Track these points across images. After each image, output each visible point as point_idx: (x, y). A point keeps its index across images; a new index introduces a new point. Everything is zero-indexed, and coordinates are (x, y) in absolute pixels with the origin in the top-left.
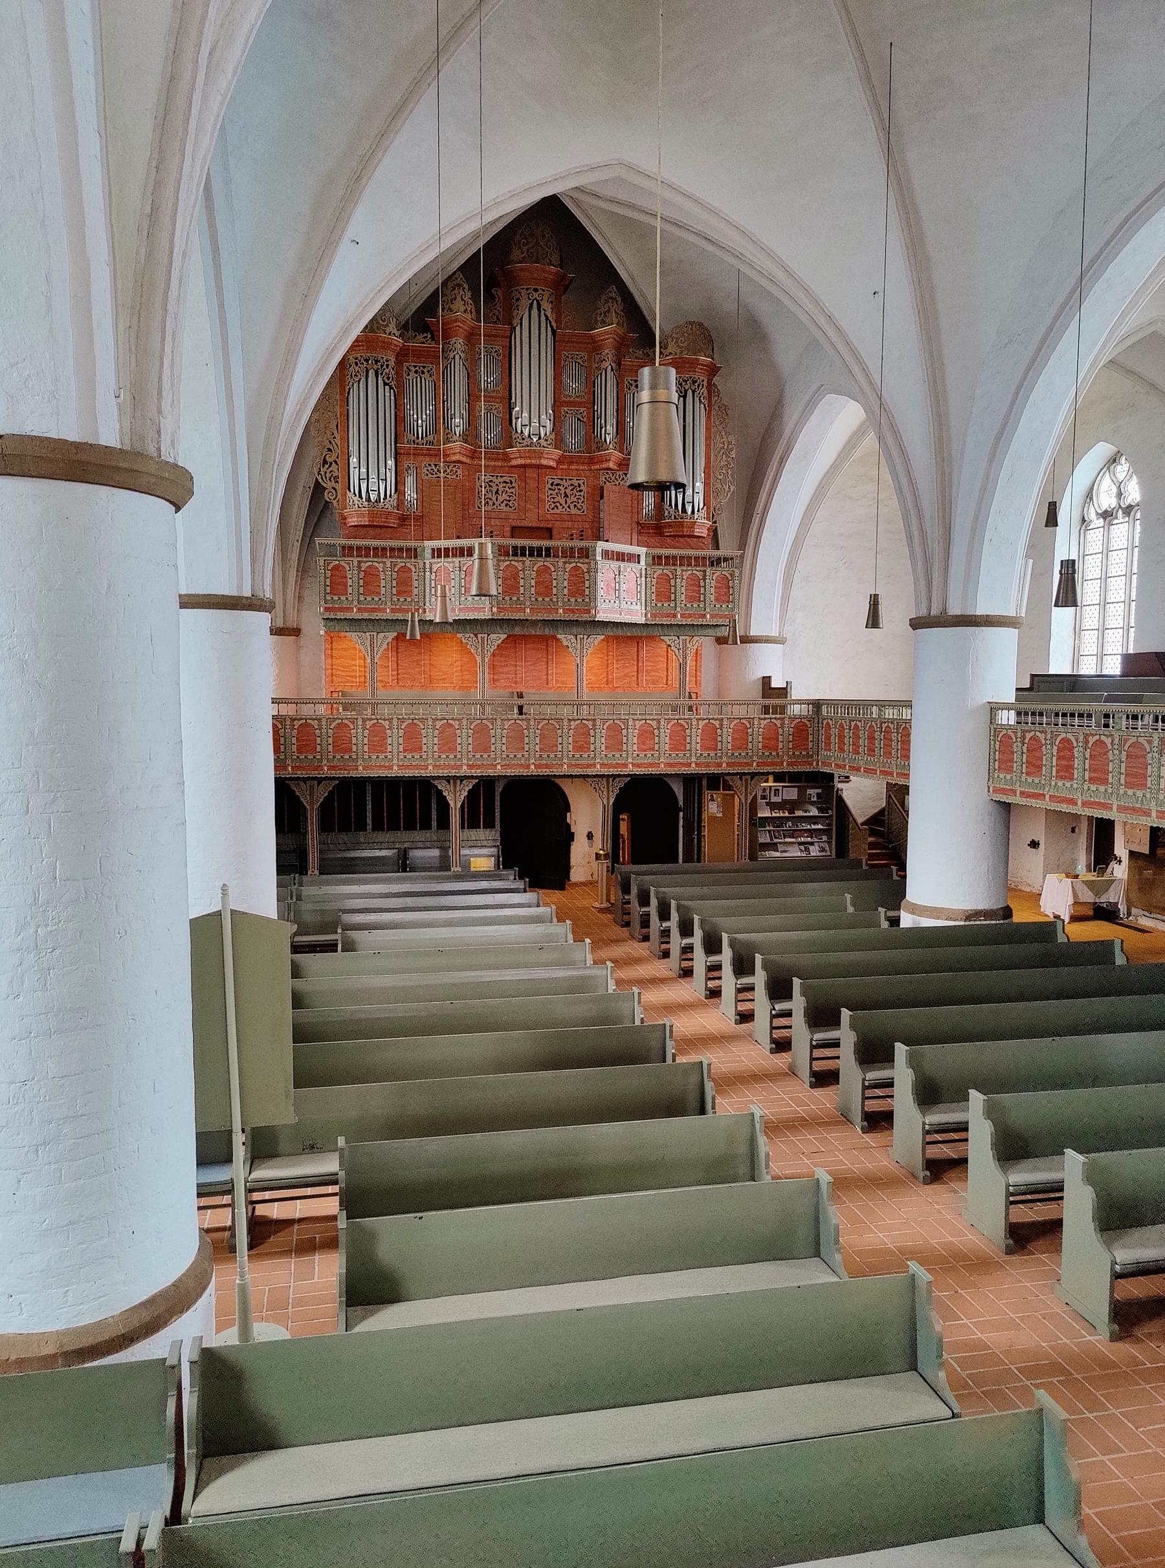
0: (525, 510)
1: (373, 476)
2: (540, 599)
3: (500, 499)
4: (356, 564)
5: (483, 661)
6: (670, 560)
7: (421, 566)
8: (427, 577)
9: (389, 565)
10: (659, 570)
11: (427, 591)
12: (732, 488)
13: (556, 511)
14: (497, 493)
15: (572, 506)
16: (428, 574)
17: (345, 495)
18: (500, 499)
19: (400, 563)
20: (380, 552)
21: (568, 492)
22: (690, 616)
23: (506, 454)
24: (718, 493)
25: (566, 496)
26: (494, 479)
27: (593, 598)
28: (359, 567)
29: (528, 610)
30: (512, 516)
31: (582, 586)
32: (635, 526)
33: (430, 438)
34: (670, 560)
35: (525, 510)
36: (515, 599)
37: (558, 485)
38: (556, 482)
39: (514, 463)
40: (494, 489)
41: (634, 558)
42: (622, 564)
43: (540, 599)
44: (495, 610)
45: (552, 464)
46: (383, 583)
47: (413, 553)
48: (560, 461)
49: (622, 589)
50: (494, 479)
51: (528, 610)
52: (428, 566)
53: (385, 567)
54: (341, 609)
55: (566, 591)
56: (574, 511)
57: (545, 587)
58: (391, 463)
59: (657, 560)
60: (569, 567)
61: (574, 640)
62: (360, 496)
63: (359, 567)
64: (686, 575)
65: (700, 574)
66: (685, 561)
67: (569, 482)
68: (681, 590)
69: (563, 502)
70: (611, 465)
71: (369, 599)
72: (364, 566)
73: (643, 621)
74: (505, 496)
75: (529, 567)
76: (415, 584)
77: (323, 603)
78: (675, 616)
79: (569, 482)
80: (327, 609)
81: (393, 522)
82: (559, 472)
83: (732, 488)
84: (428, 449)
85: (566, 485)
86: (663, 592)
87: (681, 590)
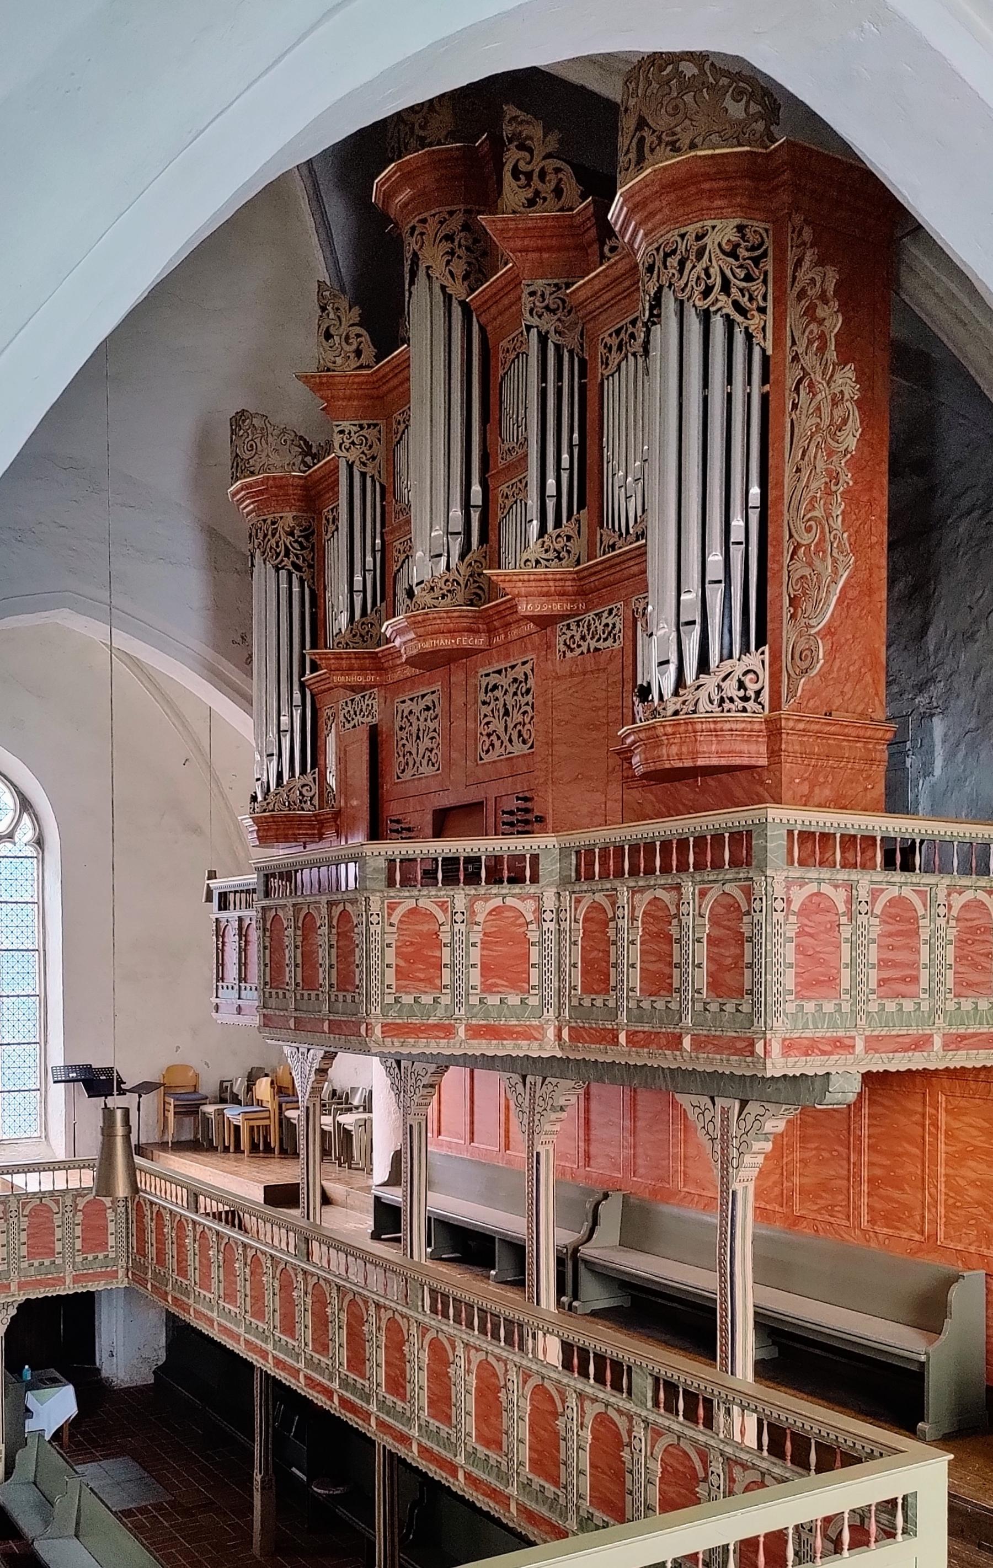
13: (493, 756)
70: (525, 608)
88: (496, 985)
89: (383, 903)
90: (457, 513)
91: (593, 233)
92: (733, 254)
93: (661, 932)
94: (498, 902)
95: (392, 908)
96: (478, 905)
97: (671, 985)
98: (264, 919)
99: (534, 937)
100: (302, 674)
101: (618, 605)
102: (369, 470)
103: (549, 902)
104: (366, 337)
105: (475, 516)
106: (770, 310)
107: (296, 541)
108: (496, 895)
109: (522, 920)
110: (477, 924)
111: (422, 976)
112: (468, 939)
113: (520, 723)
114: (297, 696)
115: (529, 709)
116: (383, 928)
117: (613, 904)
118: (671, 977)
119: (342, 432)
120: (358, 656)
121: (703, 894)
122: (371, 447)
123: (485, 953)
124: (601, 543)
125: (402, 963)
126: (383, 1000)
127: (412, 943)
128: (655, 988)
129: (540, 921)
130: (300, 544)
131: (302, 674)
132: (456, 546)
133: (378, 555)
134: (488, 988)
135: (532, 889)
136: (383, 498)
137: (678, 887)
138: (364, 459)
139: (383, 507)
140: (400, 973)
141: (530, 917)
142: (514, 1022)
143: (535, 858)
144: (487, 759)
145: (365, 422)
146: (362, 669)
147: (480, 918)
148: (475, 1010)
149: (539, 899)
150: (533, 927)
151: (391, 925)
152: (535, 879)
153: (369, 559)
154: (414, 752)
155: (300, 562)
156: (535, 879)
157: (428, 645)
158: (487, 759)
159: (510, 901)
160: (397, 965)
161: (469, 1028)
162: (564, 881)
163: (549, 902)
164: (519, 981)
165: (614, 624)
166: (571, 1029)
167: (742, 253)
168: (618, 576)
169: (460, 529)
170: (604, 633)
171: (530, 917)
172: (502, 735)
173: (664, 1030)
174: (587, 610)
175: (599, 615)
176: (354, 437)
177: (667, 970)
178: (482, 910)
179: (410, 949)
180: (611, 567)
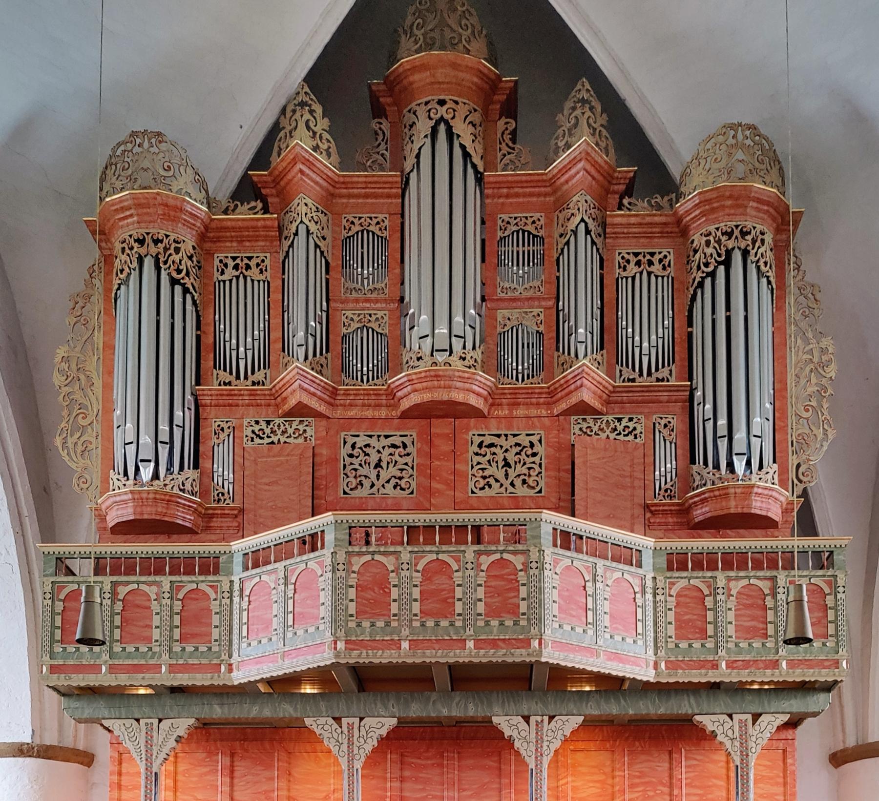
0: (429, 492)
1: (146, 439)
2: (430, 624)
3: (384, 475)
4: (107, 588)
5: (350, 767)
6: (704, 562)
7: (226, 588)
8: (236, 606)
9: (166, 587)
10: (682, 581)
11: (236, 631)
12: (831, 434)
13: (487, 492)
14: (378, 465)
15: (518, 482)
16: (236, 599)
17: (106, 480)
18: (384, 475)
19: (189, 583)
20: (155, 566)
21: (511, 457)
22: (747, 664)
23: (391, 393)
24: (803, 442)
25: (507, 464)
26: (373, 442)
27: (537, 618)
28: (114, 593)
29: (405, 645)
30: (405, 505)
31: (510, 595)
32: (639, 511)
33: (259, 376)
34: (704, 562)
35: (429, 492)
36: (380, 624)
37: (491, 445)
38: (488, 440)
39: (405, 404)
40: (374, 458)
41: (628, 557)
42: (600, 563)
43: (430, 624)
44: (341, 645)
45: (473, 400)
46: (156, 621)
47: (210, 566)
48: (494, 397)
49: (603, 612)
50: (373, 442)
51: (405, 645)
52: (236, 587)
53: (156, 589)
54: (80, 669)
55: (481, 607)
56: (522, 491)
57: (438, 601)
58: (183, 416)
59: (677, 562)
60: (485, 561)
61: (523, 725)
62: (126, 474)
63: (114, 593)
64: (736, 587)
65: (765, 586)
67: (512, 441)
68: (728, 615)
71: (130, 649)
72: (123, 591)
73: (648, 675)
74: (393, 471)
75: (406, 566)
76: (215, 620)
77: (47, 658)
78: (715, 666)
79: (512, 441)
80: (53, 669)
81: (184, 518)
82: (493, 422)
83: (831, 434)
84: (252, 393)
85: (506, 445)
86: (693, 618)
87: (728, 615)
91: (622, 188)
95: (556, 562)
101: (639, 417)
103: (649, 583)
111: (574, 613)
113: (525, 475)
115: (536, 467)
124: (621, 375)
125: (562, 602)
127: (568, 590)
128: (748, 636)
129: (644, 592)
135: (640, 571)
137: (773, 579)
144: (480, 494)
149: (643, 578)
154: (373, 475)
156: (639, 565)
158: (480, 494)
165: (635, 429)
170: (624, 431)
172: (502, 479)
173: (763, 658)
179: (566, 594)
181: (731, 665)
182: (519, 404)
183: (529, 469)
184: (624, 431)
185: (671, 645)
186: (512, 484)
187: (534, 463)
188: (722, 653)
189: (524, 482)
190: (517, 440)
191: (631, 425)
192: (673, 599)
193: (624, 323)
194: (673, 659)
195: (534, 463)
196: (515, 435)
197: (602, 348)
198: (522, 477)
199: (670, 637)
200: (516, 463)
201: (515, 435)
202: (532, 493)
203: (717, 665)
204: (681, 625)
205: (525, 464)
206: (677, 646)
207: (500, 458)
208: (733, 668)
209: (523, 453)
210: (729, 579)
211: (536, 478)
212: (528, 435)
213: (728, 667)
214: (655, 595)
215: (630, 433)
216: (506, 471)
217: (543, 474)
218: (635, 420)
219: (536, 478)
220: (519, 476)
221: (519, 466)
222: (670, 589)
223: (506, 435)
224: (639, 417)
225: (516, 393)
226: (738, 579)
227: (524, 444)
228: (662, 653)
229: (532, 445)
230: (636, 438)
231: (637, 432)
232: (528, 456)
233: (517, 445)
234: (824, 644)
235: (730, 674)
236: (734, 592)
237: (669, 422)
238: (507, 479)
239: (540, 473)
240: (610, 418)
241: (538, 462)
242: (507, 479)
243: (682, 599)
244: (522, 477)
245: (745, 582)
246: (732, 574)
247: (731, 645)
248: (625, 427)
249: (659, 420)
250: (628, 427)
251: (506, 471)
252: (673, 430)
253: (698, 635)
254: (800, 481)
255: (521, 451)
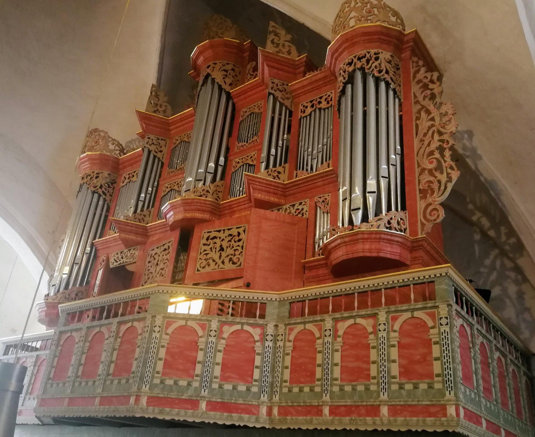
6: (317, 307)
15: (227, 261)
21: (225, 244)
22: (349, 410)
25: (222, 249)
64: (342, 327)
66: (343, 303)
67: (227, 233)
69: (216, 256)
78: (318, 411)
79: (227, 233)
88: (229, 377)
89: (164, 320)
90: (212, 165)
92: (390, 62)
93: (357, 346)
94: (238, 327)
96: (226, 328)
97: (369, 375)
98: (59, 339)
99: (258, 350)
100: (94, 238)
101: (306, 200)
102: (159, 155)
103: (270, 330)
104: (169, 107)
105: (220, 169)
106: (402, 86)
107: (107, 183)
108: (238, 323)
109: (252, 339)
110: (223, 339)
111: (181, 367)
112: (216, 347)
113: (232, 255)
114: (88, 249)
116: (161, 336)
117: (320, 330)
118: (369, 370)
119: (149, 138)
120: (137, 226)
121: (395, 319)
122: (161, 147)
123: (225, 357)
126: (152, 381)
130: (109, 185)
131: (94, 238)
132: (209, 178)
133: (155, 189)
134: (224, 378)
135: (261, 321)
136: (162, 167)
138: (157, 150)
139: (161, 171)
140: (167, 365)
141: (257, 338)
142: (241, 401)
143: (263, 305)
145: (160, 138)
146: (136, 234)
147: (225, 335)
148: (215, 392)
149: (263, 327)
150: (258, 344)
151: (167, 334)
152: (262, 316)
153: (150, 189)
155: (106, 192)
156: (262, 316)
157: (189, 215)
159: (246, 328)
160: (165, 359)
161: (209, 403)
162: (280, 318)
163: (270, 330)
164: (245, 375)
165: (303, 209)
166: (280, 407)
167: (392, 63)
168: (312, 186)
169: (213, 172)
170: (295, 212)
171: (257, 338)
173: (365, 403)
174: (286, 204)
175: (294, 206)
176: (154, 142)
177: (364, 366)
178: (228, 331)
180: (308, 181)
181: (334, 411)
182: (235, 212)
183: (235, 250)
184: (295, 212)
185: (285, 390)
186: (223, 263)
187: (238, 246)
188: (326, 398)
189: (231, 260)
190: (230, 232)
191: (300, 207)
192: (291, 344)
193: (303, 143)
194: (284, 404)
195: (238, 246)
196: (229, 229)
197: (286, 162)
198: (230, 256)
199: (286, 381)
200: (227, 247)
201: (229, 229)
202: (234, 267)
203: (321, 411)
204: (295, 368)
205: (233, 247)
206: (290, 391)
207: (218, 246)
208: (336, 415)
209: (233, 241)
210: (336, 321)
211: (239, 256)
212: (237, 228)
213: (331, 413)
214: (275, 341)
215: (299, 213)
216: (221, 253)
217: (243, 253)
218: (303, 204)
219: (239, 256)
220: (228, 256)
221: (229, 249)
222: (289, 334)
223: (224, 230)
224: (306, 200)
225: (230, 205)
226: (344, 319)
227: (234, 234)
228: (276, 398)
229: (239, 234)
230: (303, 215)
231: (304, 211)
232: (235, 242)
233: (230, 235)
234: (430, 387)
235: (332, 422)
236: (341, 333)
237: (326, 199)
238: (220, 259)
239: (241, 252)
240: (288, 206)
241: (241, 245)
242: (220, 259)
243: (298, 344)
244: (230, 256)
245: (351, 322)
246: (337, 315)
247: (336, 389)
248: (296, 210)
249: (319, 199)
250: (298, 209)
251: (221, 253)
252: (328, 204)
253: (308, 379)
254: (428, 220)
255: (232, 239)
